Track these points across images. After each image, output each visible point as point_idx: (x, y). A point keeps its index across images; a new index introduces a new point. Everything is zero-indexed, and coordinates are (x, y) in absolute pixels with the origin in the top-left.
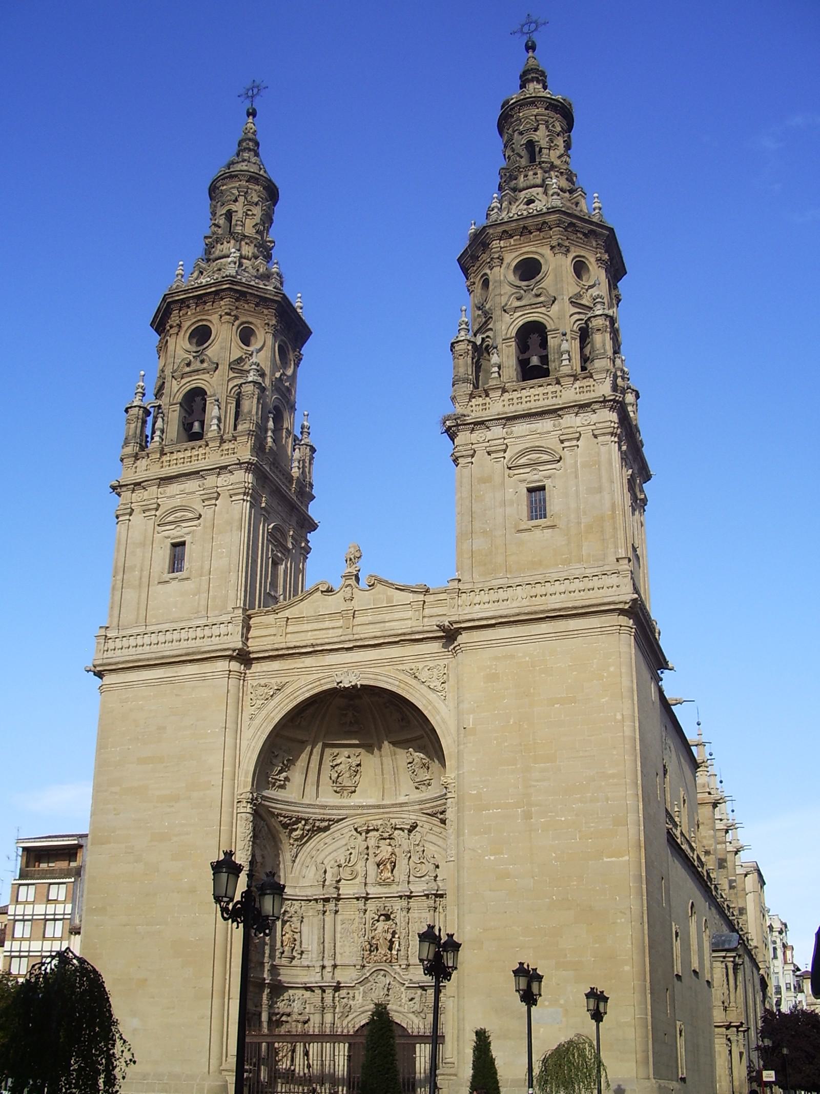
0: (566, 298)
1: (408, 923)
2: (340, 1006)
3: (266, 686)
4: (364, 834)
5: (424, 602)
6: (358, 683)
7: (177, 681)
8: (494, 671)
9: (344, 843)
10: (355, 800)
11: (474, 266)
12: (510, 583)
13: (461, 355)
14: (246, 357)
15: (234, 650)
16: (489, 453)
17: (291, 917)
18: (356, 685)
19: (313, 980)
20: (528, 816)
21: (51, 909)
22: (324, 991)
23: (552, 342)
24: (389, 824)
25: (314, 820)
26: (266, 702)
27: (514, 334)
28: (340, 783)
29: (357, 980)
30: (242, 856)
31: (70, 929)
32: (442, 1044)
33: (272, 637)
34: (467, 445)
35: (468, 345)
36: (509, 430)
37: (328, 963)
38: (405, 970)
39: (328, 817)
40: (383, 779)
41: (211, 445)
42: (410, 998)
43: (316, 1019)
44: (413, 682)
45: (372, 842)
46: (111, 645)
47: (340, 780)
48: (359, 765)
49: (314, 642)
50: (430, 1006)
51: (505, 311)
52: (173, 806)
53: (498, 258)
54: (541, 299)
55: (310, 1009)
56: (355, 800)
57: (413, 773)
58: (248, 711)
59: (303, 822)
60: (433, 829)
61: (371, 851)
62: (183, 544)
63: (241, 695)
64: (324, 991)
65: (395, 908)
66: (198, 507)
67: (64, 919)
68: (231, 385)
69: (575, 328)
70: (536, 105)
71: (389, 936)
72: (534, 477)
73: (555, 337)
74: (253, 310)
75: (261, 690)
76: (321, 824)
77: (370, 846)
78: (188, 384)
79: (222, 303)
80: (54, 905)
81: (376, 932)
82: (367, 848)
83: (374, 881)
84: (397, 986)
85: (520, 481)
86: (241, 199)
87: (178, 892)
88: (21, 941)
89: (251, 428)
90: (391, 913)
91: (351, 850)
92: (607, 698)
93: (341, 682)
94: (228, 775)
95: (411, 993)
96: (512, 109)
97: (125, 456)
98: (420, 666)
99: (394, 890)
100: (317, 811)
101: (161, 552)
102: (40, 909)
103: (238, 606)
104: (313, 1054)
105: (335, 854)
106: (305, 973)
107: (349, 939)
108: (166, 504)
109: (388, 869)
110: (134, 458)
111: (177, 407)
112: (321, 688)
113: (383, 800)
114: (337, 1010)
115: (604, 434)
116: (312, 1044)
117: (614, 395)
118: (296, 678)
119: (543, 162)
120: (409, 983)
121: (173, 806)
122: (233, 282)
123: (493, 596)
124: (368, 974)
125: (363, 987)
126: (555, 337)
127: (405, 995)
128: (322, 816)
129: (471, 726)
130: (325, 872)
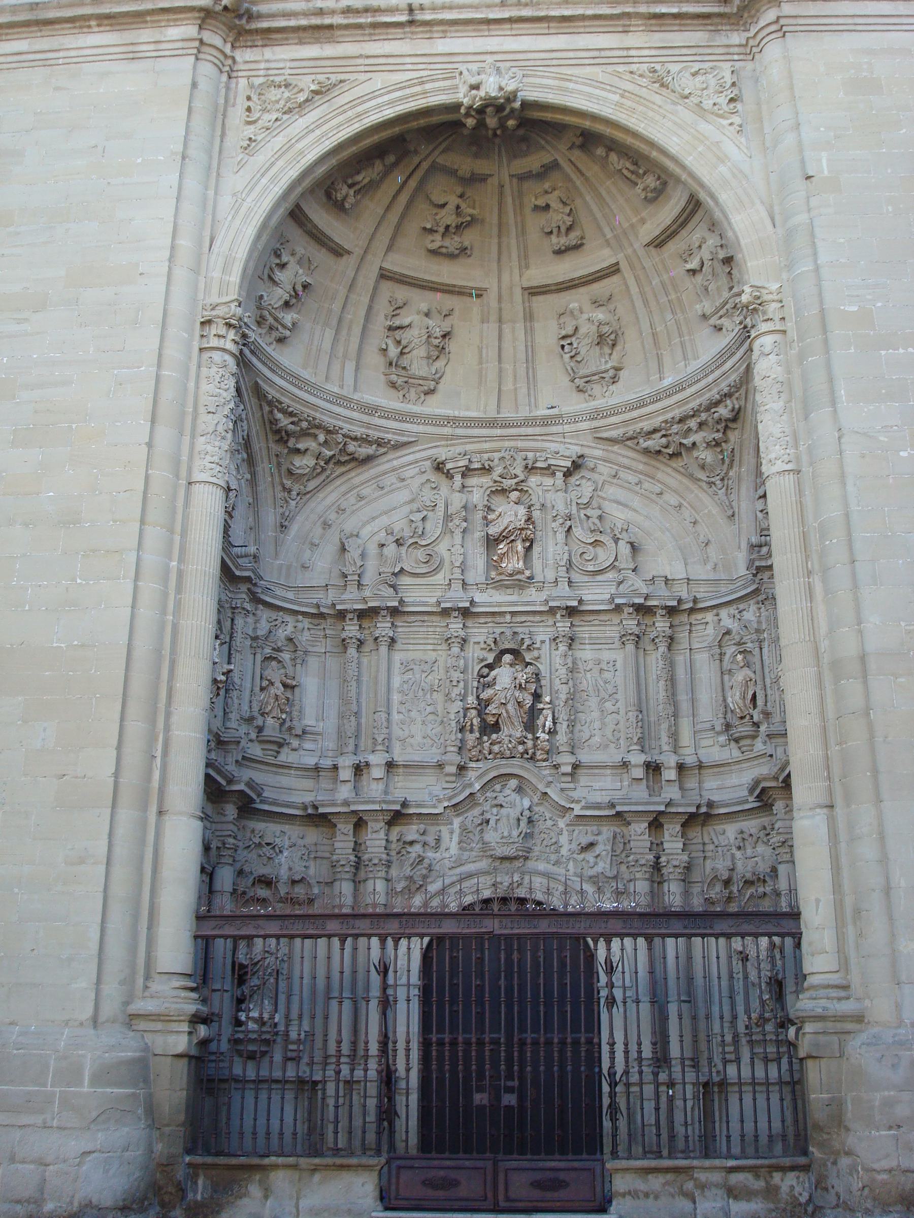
3: (286, 86)
4: (458, 478)
7: (61, 61)
10: (434, 406)
17: (279, 650)
26: (286, 117)
28: (404, 368)
30: (209, 448)
38: (569, 779)
40: (500, 370)
45: (477, 497)
47: (405, 362)
48: (444, 336)
50: (643, 862)
52: (26, 320)
58: (238, 132)
60: (621, 474)
65: (538, 639)
71: (528, 701)
76: (359, 449)
83: (483, 580)
87: (26, 525)
90: (529, 649)
98: (674, 68)
99: (534, 598)
100: (355, 415)
105: (384, 521)
107: (423, 705)
112: (424, 101)
113: (498, 413)
116: (403, 942)
118: (363, 77)
120: (583, 808)
121: (26, 320)
124: (477, 786)
125: (460, 819)
128: (363, 430)
129: (826, 172)
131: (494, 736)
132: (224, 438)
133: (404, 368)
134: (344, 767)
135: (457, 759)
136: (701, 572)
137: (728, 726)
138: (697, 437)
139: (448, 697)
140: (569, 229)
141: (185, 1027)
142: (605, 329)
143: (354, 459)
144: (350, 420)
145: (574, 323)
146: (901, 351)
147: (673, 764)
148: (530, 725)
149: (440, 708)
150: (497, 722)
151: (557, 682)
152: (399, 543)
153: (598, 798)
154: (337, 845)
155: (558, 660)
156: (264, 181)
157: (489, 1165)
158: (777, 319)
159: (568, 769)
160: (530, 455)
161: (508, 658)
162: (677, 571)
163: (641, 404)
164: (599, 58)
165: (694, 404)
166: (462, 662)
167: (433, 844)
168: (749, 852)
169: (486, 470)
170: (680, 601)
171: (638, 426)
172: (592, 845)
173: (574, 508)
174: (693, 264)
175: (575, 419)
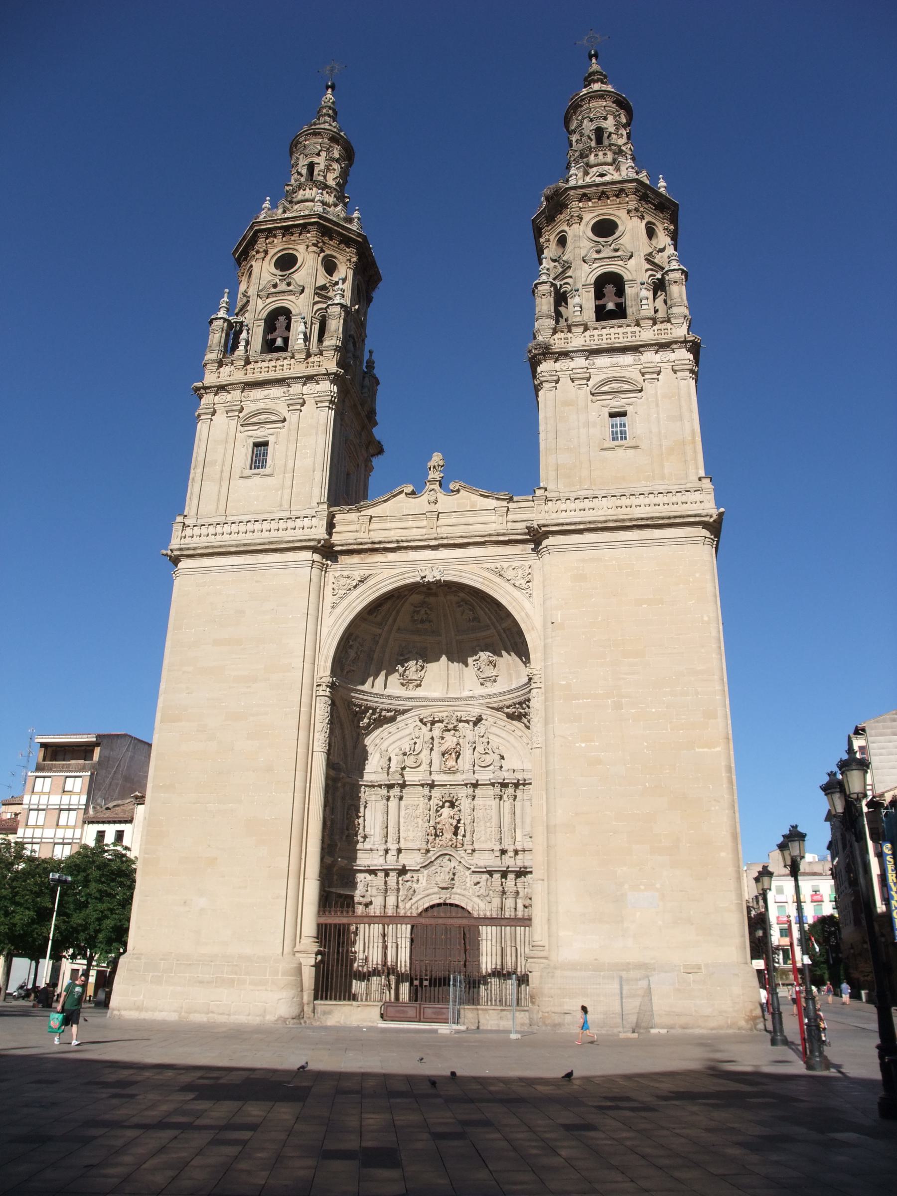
0: (642, 255)
1: (474, 811)
2: (404, 889)
3: (348, 577)
5: (508, 510)
6: (442, 579)
8: (581, 572)
9: (408, 733)
10: (420, 693)
11: (548, 226)
12: (596, 493)
13: (544, 295)
14: (330, 286)
15: (319, 541)
16: (573, 380)
18: (440, 580)
19: (375, 862)
20: (618, 706)
21: (66, 799)
22: (387, 875)
23: (628, 291)
24: (454, 716)
25: (382, 710)
26: (348, 592)
27: (593, 281)
29: (422, 863)
31: (83, 818)
32: (528, 926)
33: (355, 533)
34: (551, 371)
35: (551, 287)
36: (591, 362)
37: (393, 847)
38: (470, 855)
39: (395, 707)
40: (448, 674)
41: (297, 356)
42: (475, 882)
43: (378, 901)
44: (498, 580)
46: (188, 531)
49: (400, 539)
51: (584, 261)
53: (578, 216)
54: (618, 254)
55: (371, 891)
56: (420, 693)
57: (478, 670)
59: (371, 711)
60: (498, 722)
61: (436, 741)
62: (266, 444)
63: (322, 584)
64: (387, 875)
65: (460, 795)
66: (284, 411)
67: (78, 809)
68: (316, 307)
69: (649, 281)
70: (605, 99)
71: (455, 823)
72: (617, 404)
73: (632, 287)
74: (336, 246)
75: (343, 581)
77: (434, 736)
78: (274, 303)
79: (308, 235)
80: (69, 796)
81: (442, 817)
82: (432, 738)
84: (462, 870)
85: (603, 406)
86: (323, 154)
88: (34, 828)
89: (338, 344)
90: (457, 800)
91: (415, 740)
92: (693, 601)
93: (425, 577)
94: (308, 659)
95: (476, 878)
96: (582, 100)
97: (210, 362)
98: (505, 565)
99: (459, 778)
101: (244, 450)
102: (55, 799)
103: (322, 501)
104: (369, 937)
106: (367, 856)
108: (249, 408)
110: (217, 364)
111: (262, 323)
113: (447, 693)
114: (400, 894)
115: (683, 370)
117: (694, 336)
118: (380, 571)
119: (613, 145)
120: (475, 868)
122: (320, 217)
123: (579, 504)
125: (427, 871)
126: (632, 287)
127: (471, 879)
129: (559, 621)
130: (390, 760)
132: (326, 732)
141: (314, 956)
143: (387, 718)
144: (382, 703)
146: (581, 701)
148: (456, 834)
151: (467, 815)
155: (467, 805)
156: (340, 621)
157: (418, 1006)
158: (538, 682)
159: (470, 851)
162: (517, 765)
163: (504, 694)
164: (475, 560)
166: (429, 806)
167: (416, 881)
169: (441, 721)
170: (518, 780)
171: (503, 703)
172: (478, 883)
173: (477, 737)
175: (478, 697)
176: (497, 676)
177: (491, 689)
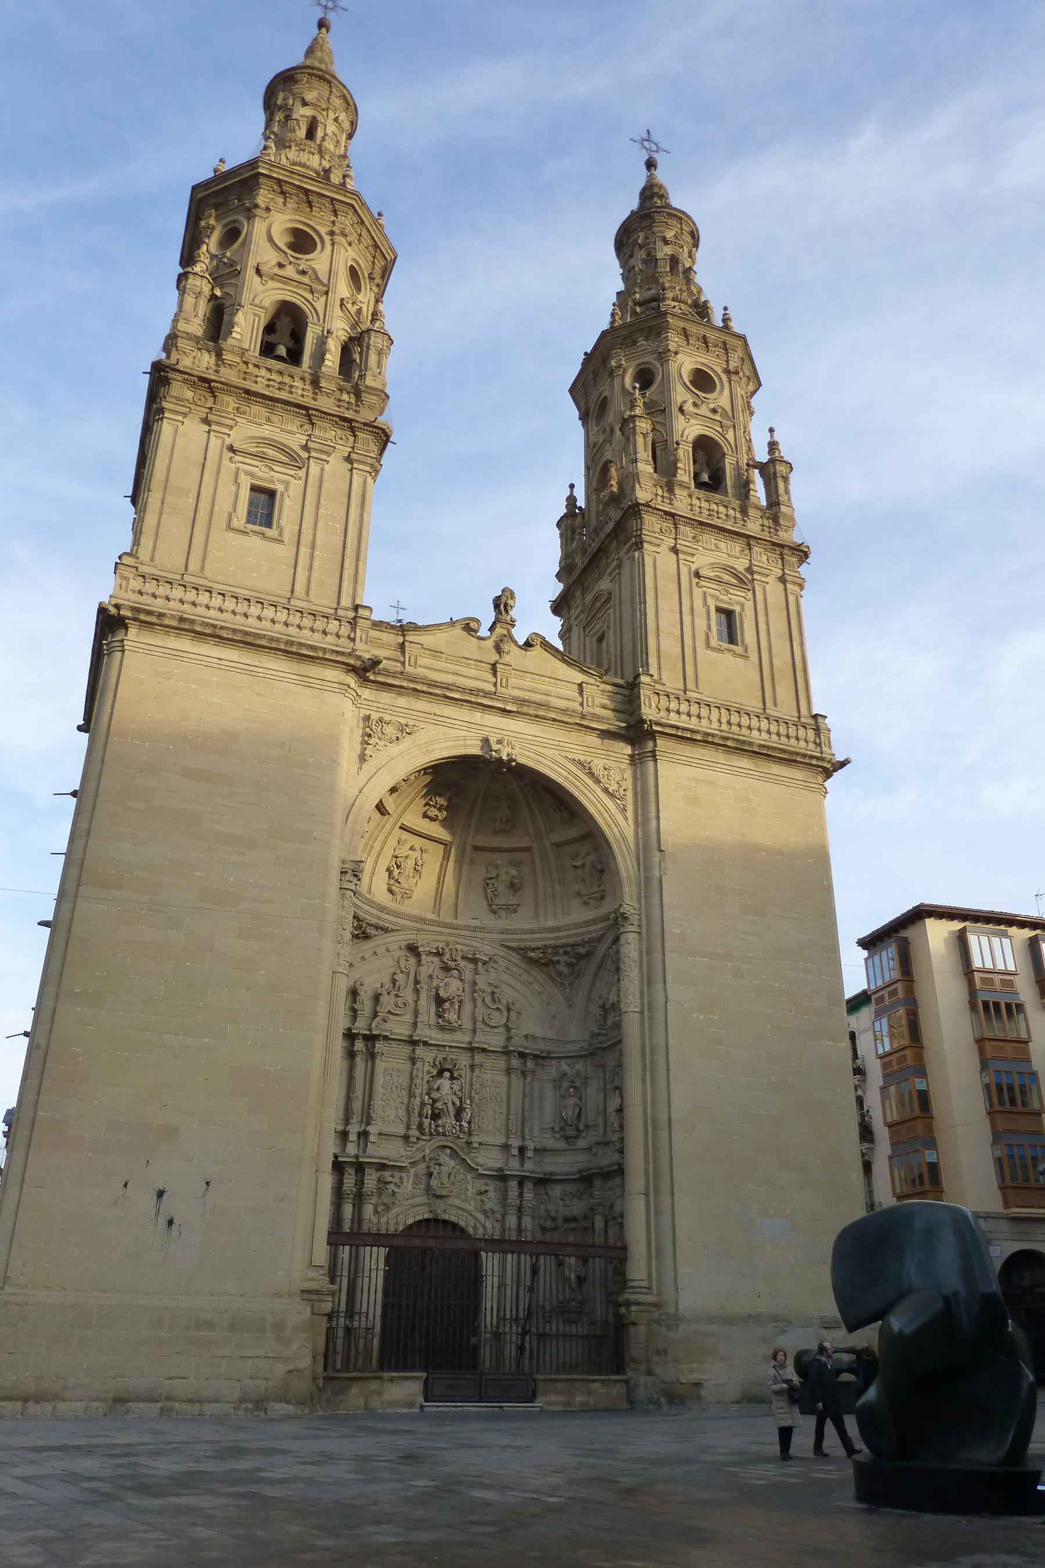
71: (458, 1103)
95: (481, 1185)
99: (462, 1038)
100: (374, 911)
109: (455, 1009)
120: (485, 1170)
131: (440, 1122)
133: (399, 883)
134: (352, 1133)
135: (416, 1133)
136: (551, 1034)
137: (561, 1129)
138: (562, 958)
139: (411, 1095)
140: (507, 821)
142: (515, 881)
144: (371, 914)
145: (497, 872)
147: (532, 1148)
148: (458, 1116)
149: (406, 1100)
150: (439, 1113)
151: (473, 1092)
152: (388, 994)
153: (490, 1164)
154: (345, 1181)
160: (466, 948)
161: (447, 1074)
163: (533, 932)
165: (565, 941)
168: (568, 1202)
171: (528, 944)
172: (487, 1191)
174: (578, 864)
176: (518, 905)
177: (505, 922)
